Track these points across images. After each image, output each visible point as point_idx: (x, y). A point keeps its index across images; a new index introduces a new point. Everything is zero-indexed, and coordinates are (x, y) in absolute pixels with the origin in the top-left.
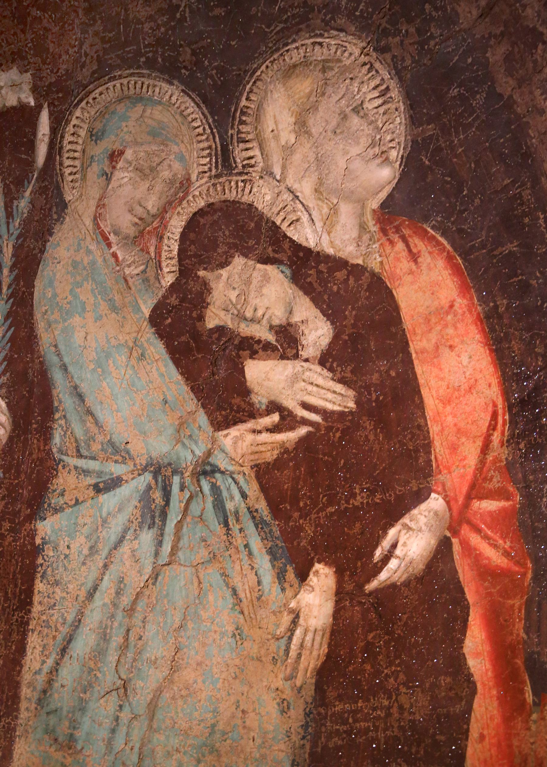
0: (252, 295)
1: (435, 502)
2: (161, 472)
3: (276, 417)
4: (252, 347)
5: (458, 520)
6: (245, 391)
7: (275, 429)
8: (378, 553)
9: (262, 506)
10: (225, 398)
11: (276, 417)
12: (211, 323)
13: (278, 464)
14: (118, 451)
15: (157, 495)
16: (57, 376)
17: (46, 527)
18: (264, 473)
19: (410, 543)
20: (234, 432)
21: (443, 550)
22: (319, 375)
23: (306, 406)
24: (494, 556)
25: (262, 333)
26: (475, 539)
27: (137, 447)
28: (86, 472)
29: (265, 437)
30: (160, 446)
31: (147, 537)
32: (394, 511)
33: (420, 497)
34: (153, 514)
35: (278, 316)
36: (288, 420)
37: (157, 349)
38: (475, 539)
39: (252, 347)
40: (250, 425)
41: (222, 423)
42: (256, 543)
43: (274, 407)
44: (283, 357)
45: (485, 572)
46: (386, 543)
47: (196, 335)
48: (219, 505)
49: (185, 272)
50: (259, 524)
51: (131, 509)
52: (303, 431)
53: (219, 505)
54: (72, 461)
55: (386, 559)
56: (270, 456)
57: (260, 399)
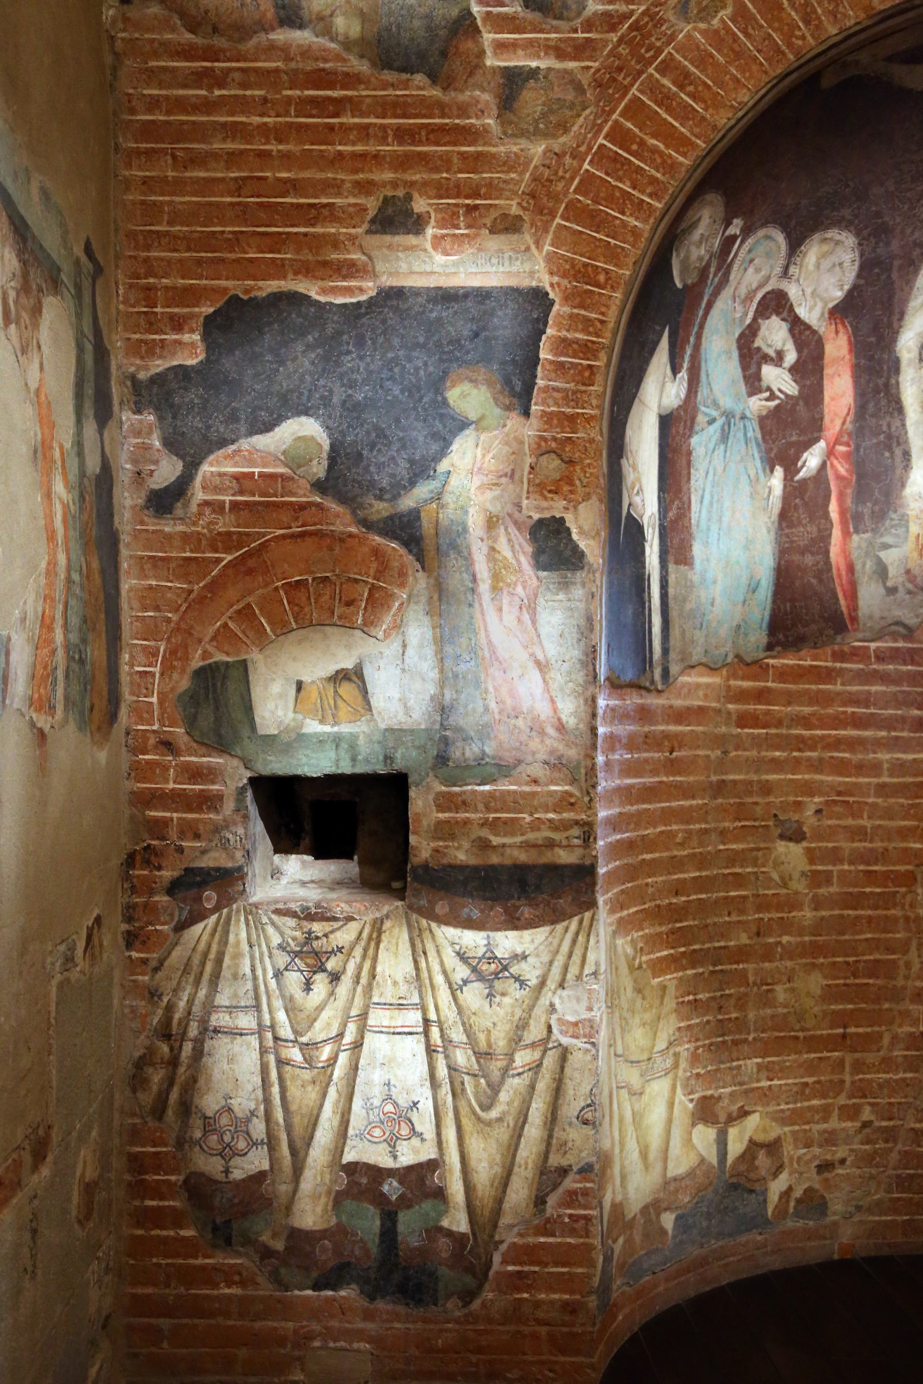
0: (775, 334)
1: (822, 444)
2: (728, 415)
3: (767, 394)
4: (766, 359)
5: (830, 452)
6: (759, 379)
7: (767, 400)
8: (800, 464)
9: (759, 436)
10: (753, 383)
11: (767, 394)
12: (756, 345)
13: (767, 417)
14: (716, 404)
15: (726, 427)
16: (703, 364)
17: (694, 440)
18: (763, 421)
19: (812, 460)
20: (754, 399)
21: (823, 465)
22: (787, 376)
23: (780, 391)
24: (842, 471)
25: (772, 353)
26: (835, 462)
27: (721, 402)
28: (706, 414)
29: (764, 403)
30: (727, 402)
31: (722, 447)
32: (808, 445)
33: (817, 440)
34: (724, 437)
35: (779, 346)
36: (772, 397)
37: (735, 354)
38: (835, 462)
39: (766, 359)
40: (759, 396)
41: (751, 394)
42: (757, 455)
43: (769, 389)
44: (776, 365)
45: (839, 477)
46: (803, 459)
47: (749, 349)
48: (745, 434)
49: (755, 319)
50: (758, 445)
51: (717, 435)
52: (777, 402)
53: (745, 434)
54: (703, 409)
55: (802, 467)
56: (764, 413)
57: (764, 385)
